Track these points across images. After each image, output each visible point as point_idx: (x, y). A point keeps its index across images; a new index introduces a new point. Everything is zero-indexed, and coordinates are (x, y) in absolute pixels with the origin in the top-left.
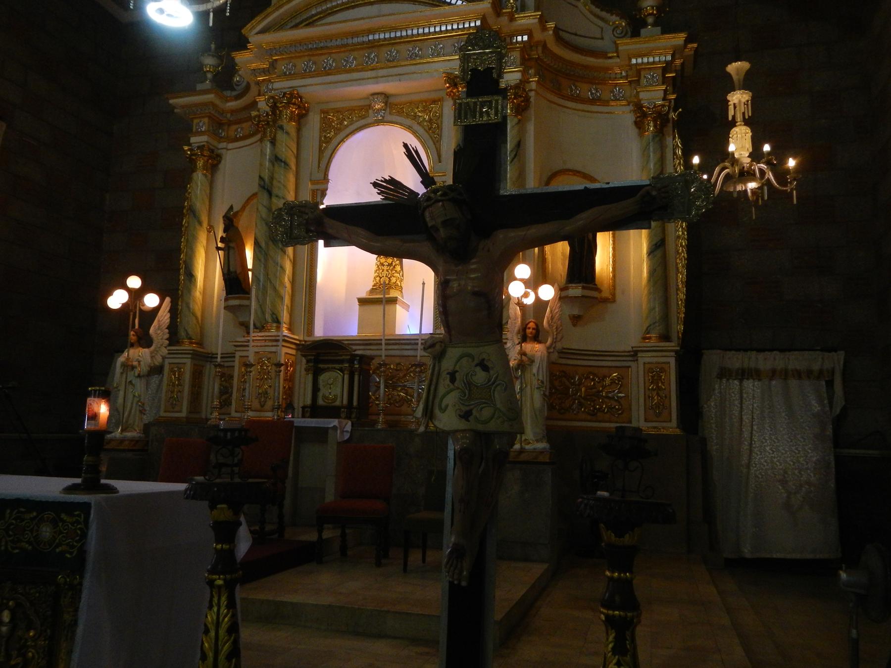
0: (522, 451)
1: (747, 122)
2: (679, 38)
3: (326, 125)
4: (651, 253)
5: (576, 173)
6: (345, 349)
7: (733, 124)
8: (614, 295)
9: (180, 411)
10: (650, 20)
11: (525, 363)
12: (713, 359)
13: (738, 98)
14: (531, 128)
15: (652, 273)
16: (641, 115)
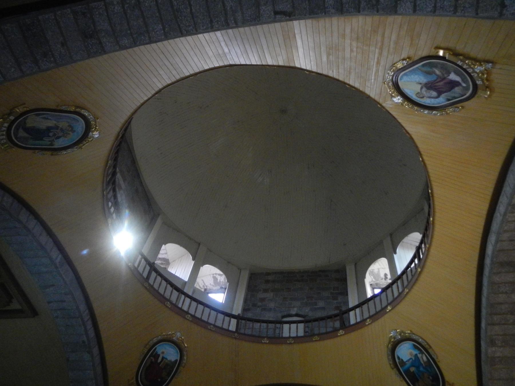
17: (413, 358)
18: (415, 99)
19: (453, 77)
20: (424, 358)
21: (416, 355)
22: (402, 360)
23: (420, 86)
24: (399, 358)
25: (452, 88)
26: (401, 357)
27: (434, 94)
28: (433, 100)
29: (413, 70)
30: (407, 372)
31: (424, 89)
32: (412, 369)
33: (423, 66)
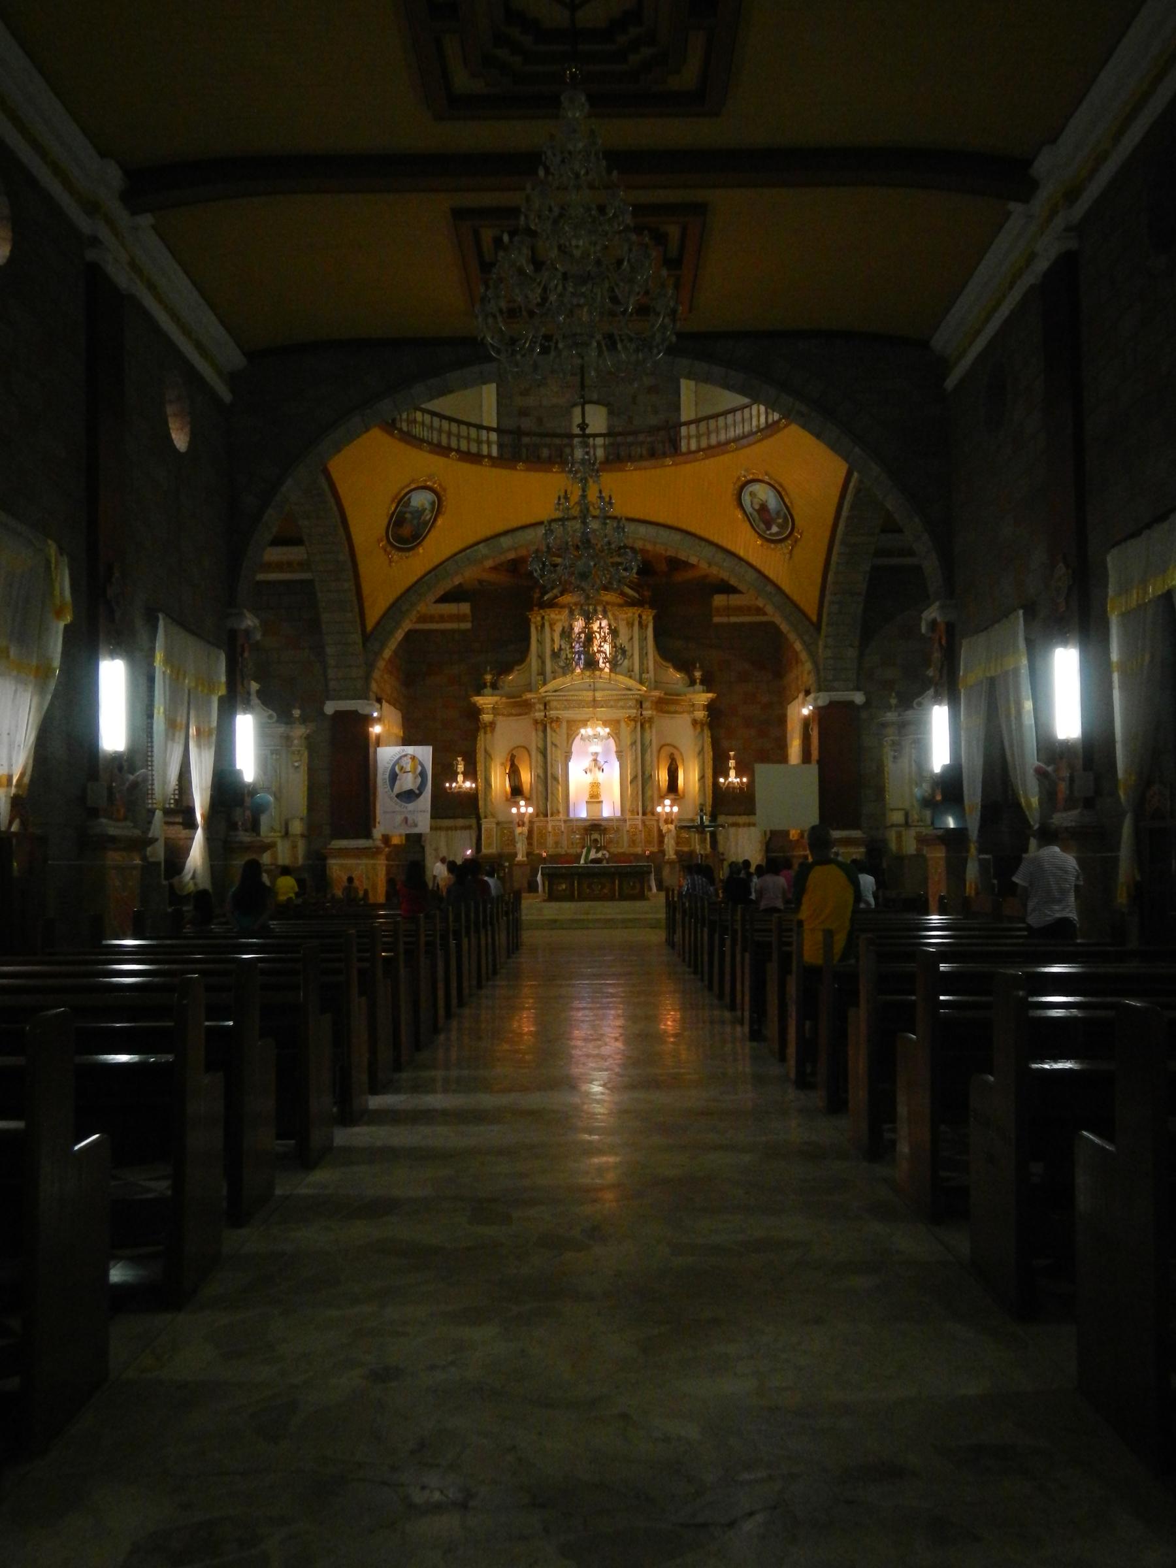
0: (669, 859)
1: (734, 768)
2: (710, 695)
3: (569, 728)
4: (699, 780)
5: (668, 745)
6: (601, 825)
7: (730, 768)
8: (684, 795)
9: (493, 848)
10: (698, 681)
11: (669, 831)
12: (721, 819)
13: (732, 763)
14: (654, 730)
15: (700, 788)
16: (695, 722)
17: (420, 509)
18: (747, 489)
19: (775, 529)
20: (428, 516)
21: (426, 509)
22: (410, 502)
23: (764, 500)
24: (409, 499)
25: (764, 522)
26: (412, 500)
27: (757, 507)
28: (750, 503)
29: (780, 504)
30: (402, 514)
31: (761, 502)
32: (408, 516)
33: (785, 514)
